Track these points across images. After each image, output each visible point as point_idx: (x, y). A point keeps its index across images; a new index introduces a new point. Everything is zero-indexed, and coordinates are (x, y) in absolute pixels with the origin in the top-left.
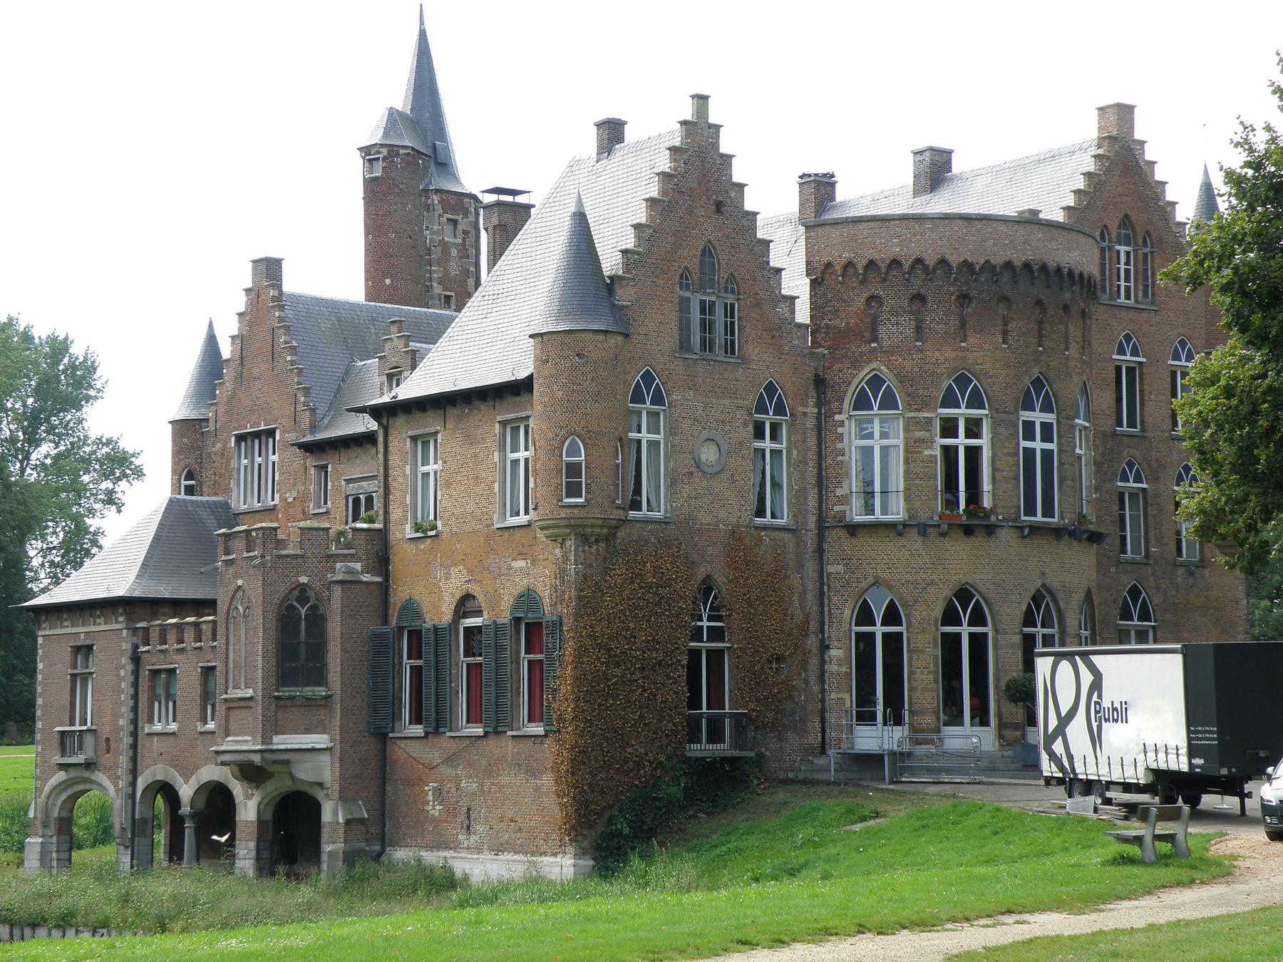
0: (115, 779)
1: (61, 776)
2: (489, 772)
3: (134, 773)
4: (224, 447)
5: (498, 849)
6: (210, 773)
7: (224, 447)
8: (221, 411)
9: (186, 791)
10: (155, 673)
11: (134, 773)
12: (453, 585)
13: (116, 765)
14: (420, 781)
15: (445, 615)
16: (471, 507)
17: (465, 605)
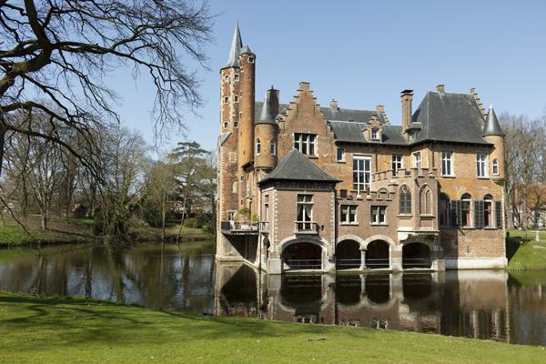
0: (329, 240)
1: (294, 237)
2: (478, 236)
3: (336, 237)
4: (289, 136)
5: (480, 256)
6: (375, 238)
7: (289, 136)
8: (286, 124)
9: (364, 244)
10: (344, 207)
11: (336, 237)
12: (463, 190)
13: (329, 234)
14: (449, 240)
15: (458, 198)
16: (467, 171)
17: (466, 196)
